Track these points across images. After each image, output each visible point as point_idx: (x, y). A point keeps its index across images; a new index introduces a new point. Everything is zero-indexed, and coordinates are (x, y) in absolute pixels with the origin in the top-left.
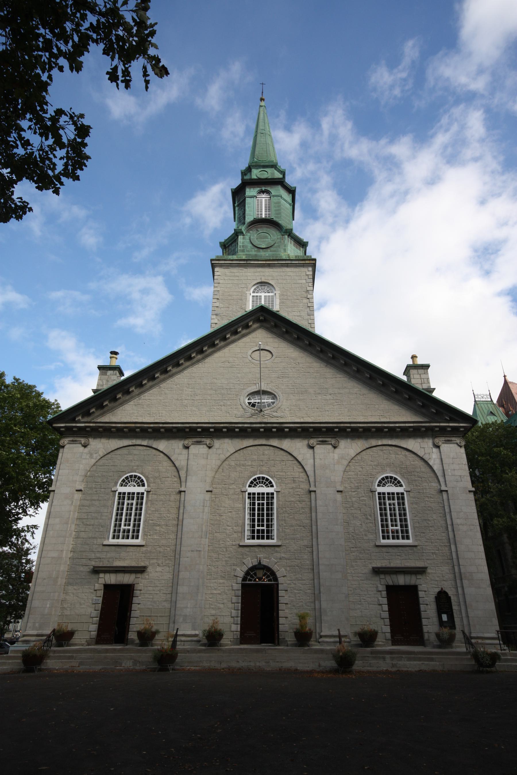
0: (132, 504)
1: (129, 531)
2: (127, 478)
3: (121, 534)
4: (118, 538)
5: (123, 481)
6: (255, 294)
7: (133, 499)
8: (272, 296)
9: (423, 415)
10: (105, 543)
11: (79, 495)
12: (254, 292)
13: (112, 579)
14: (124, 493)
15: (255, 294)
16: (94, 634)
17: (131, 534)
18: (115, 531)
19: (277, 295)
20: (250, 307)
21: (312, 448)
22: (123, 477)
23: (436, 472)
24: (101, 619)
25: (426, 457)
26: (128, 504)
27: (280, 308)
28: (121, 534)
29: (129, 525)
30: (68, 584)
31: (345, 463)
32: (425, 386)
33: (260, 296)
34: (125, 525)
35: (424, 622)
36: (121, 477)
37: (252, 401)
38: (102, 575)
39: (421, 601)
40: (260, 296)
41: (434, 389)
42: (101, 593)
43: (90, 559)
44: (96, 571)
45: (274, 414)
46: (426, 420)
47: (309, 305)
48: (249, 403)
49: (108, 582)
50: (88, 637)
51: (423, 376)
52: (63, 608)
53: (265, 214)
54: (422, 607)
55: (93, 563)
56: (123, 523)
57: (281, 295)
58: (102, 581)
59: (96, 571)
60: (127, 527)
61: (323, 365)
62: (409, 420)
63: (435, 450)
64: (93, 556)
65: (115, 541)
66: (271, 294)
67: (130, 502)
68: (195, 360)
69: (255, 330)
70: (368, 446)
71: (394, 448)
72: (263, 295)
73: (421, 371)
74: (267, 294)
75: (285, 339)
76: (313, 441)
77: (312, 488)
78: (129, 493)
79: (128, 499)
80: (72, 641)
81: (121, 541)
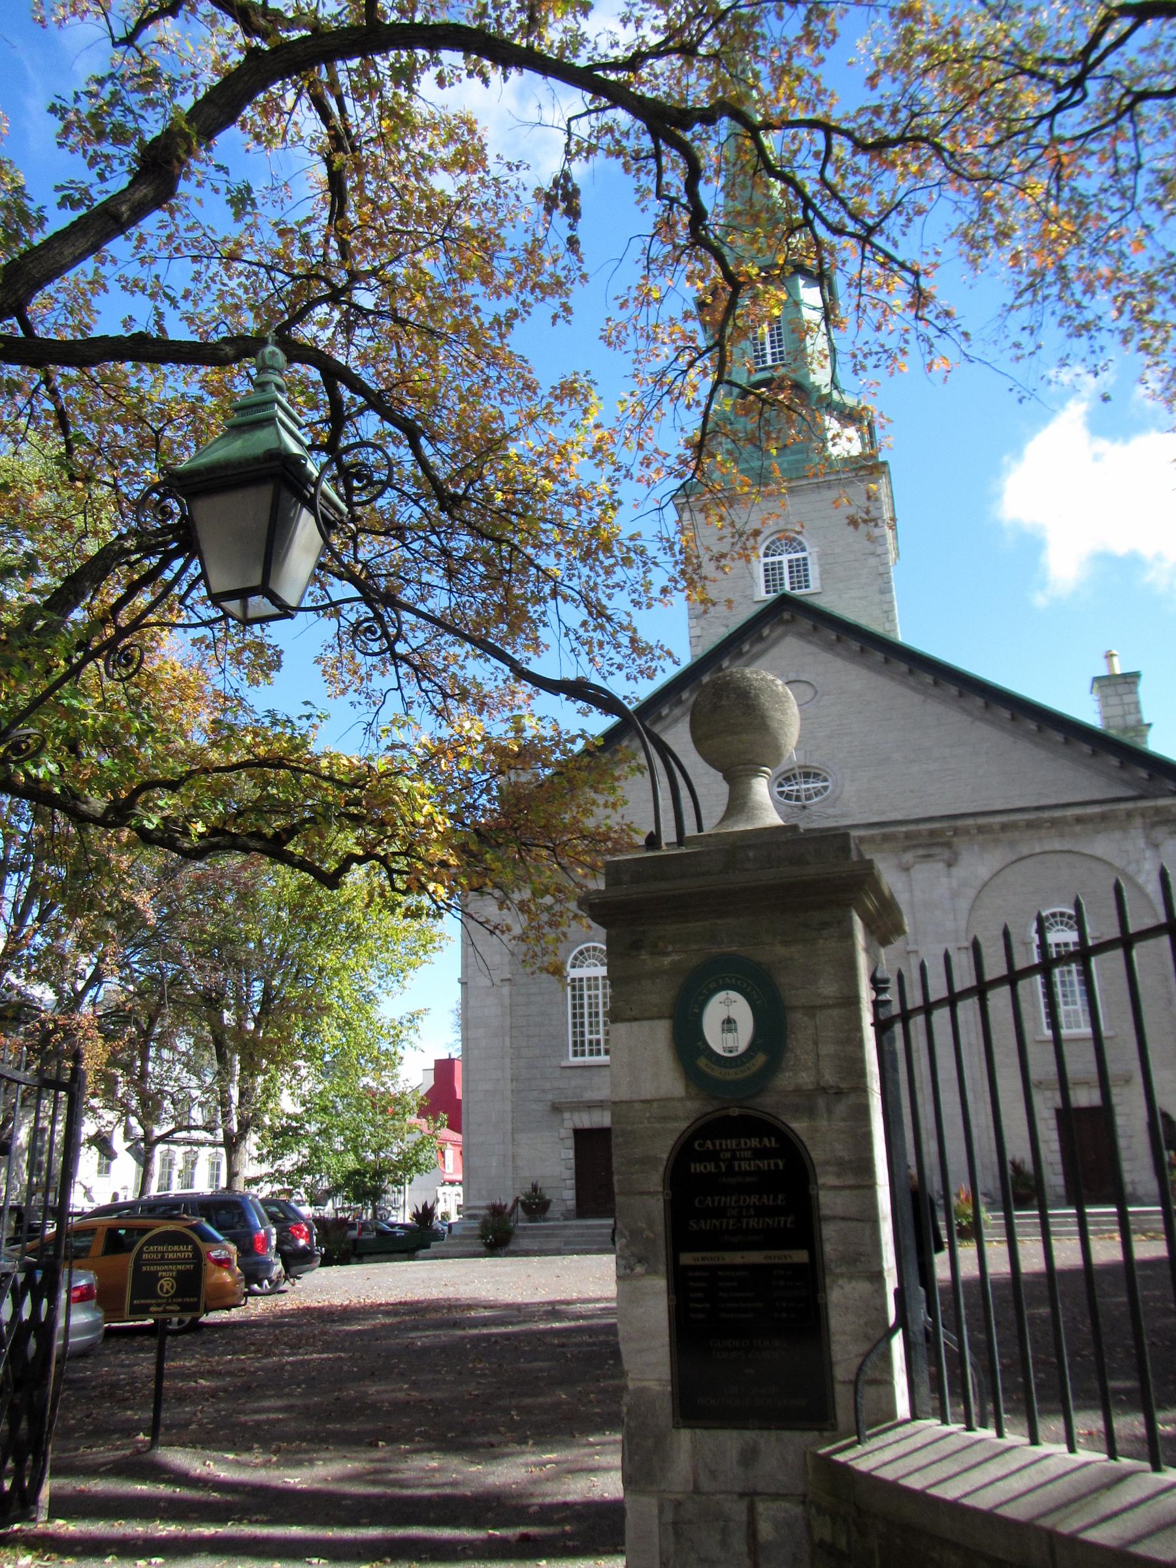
0: (597, 997)
1: (598, 1042)
2: (581, 953)
3: (587, 1048)
4: (583, 1054)
5: (576, 958)
6: (770, 560)
7: (597, 988)
8: (805, 559)
9: (1126, 783)
10: (564, 1064)
11: (506, 990)
12: (766, 555)
13: (586, 1120)
14: (581, 980)
15: (770, 560)
16: (572, 1204)
17: (602, 1047)
18: (575, 1044)
19: (815, 555)
20: (762, 595)
21: (907, 869)
22: (575, 952)
23: (1152, 895)
24: (577, 1180)
25: (1131, 869)
26: (590, 997)
27: (822, 586)
28: (587, 1048)
29: (598, 1033)
30: (514, 1131)
31: (971, 893)
32: (1131, 720)
33: (780, 563)
34: (591, 1033)
35: (1125, 1166)
36: (570, 952)
37: (786, 789)
38: (567, 1115)
39: (1120, 1131)
40: (780, 563)
41: (1149, 725)
42: (570, 1143)
43: (543, 1091)
44: (557, 1109)
45: (830, 811)
46: (1131, 793)
47: (882, 569)
48: (781, 793)
49: (579, 1126)
50: (563, 1208)
51: (1127, 699)
52: (515, 1168)
53: (773, 354)
54: (1122, 1142)
55: (550, 1097)
56: (586, 1029)
57: (822, 556)
58: (569, 1124)
59: (557, 1109)
60: (594, 1037)
61: (918, 698)
62: (1098, 796)
63: (1148, 854)
64: (548, 1085)
65: (579, 1060)
66: (800, 555)
67: (593, 992)
68: (669, 719)
69: (775, 642)
70: (1014, 858)
71: (1065, 856)
72: (785, 558)
73: (1121, 689)
74: (794, 556)
75: (838, 655)
76: (908, 857)
77: (909, 948)
78: (589, 979)
79: (589, 988)
80: (548, 1215)
81: (588, 1059)
